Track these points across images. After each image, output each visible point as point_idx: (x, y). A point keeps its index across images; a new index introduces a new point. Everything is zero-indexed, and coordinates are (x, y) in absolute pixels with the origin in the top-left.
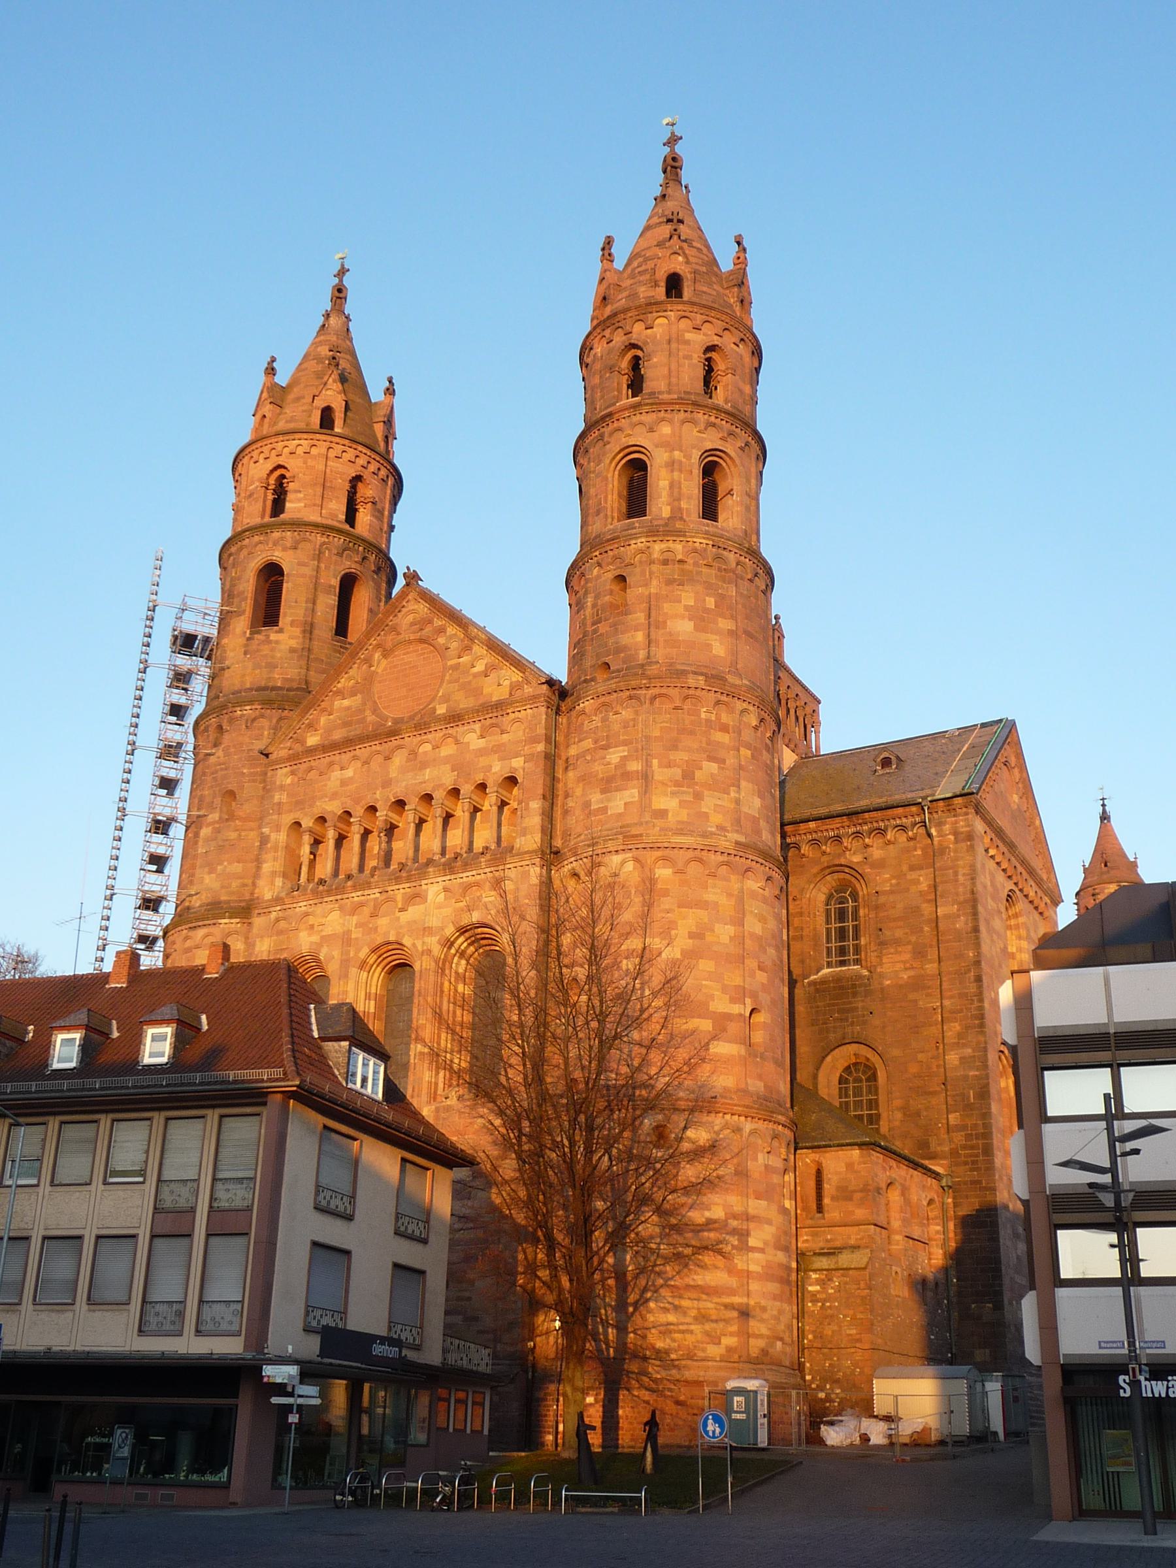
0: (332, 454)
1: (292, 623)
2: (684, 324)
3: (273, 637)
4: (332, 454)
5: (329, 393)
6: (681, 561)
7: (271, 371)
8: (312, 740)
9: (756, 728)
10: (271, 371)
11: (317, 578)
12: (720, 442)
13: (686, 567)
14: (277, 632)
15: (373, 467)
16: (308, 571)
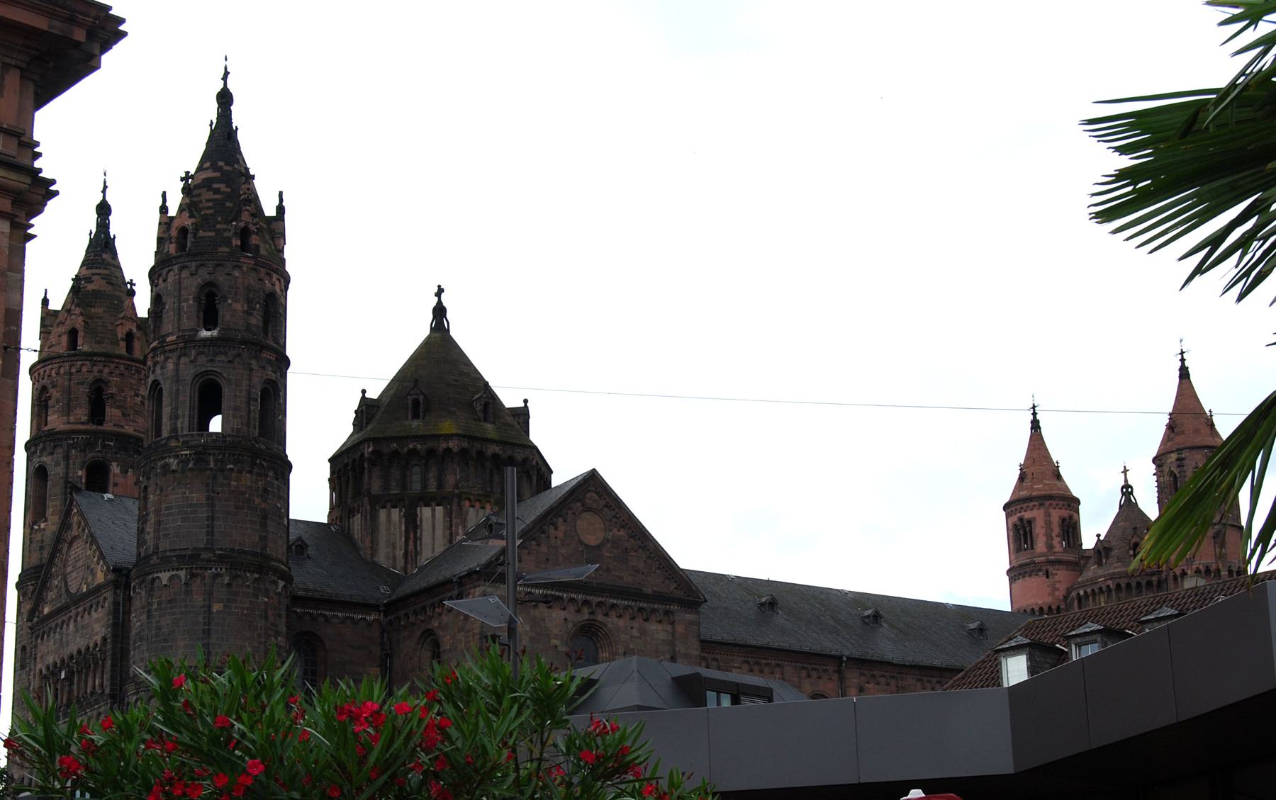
0: (74, 370)
1: (53, 514)
2: (185, 274)
3: (42, 526)
4: (74, 370)
5: (73, 317)
6: (174, 471)
7: (45, 302)
8: (46, 611)
9: (229, 585)
10: (45, 302)
11: (67, 473)
12: (210, 364)
13: (178, 475)
14: (44, 522)
15: (106, 370)
16: (60, 470)
